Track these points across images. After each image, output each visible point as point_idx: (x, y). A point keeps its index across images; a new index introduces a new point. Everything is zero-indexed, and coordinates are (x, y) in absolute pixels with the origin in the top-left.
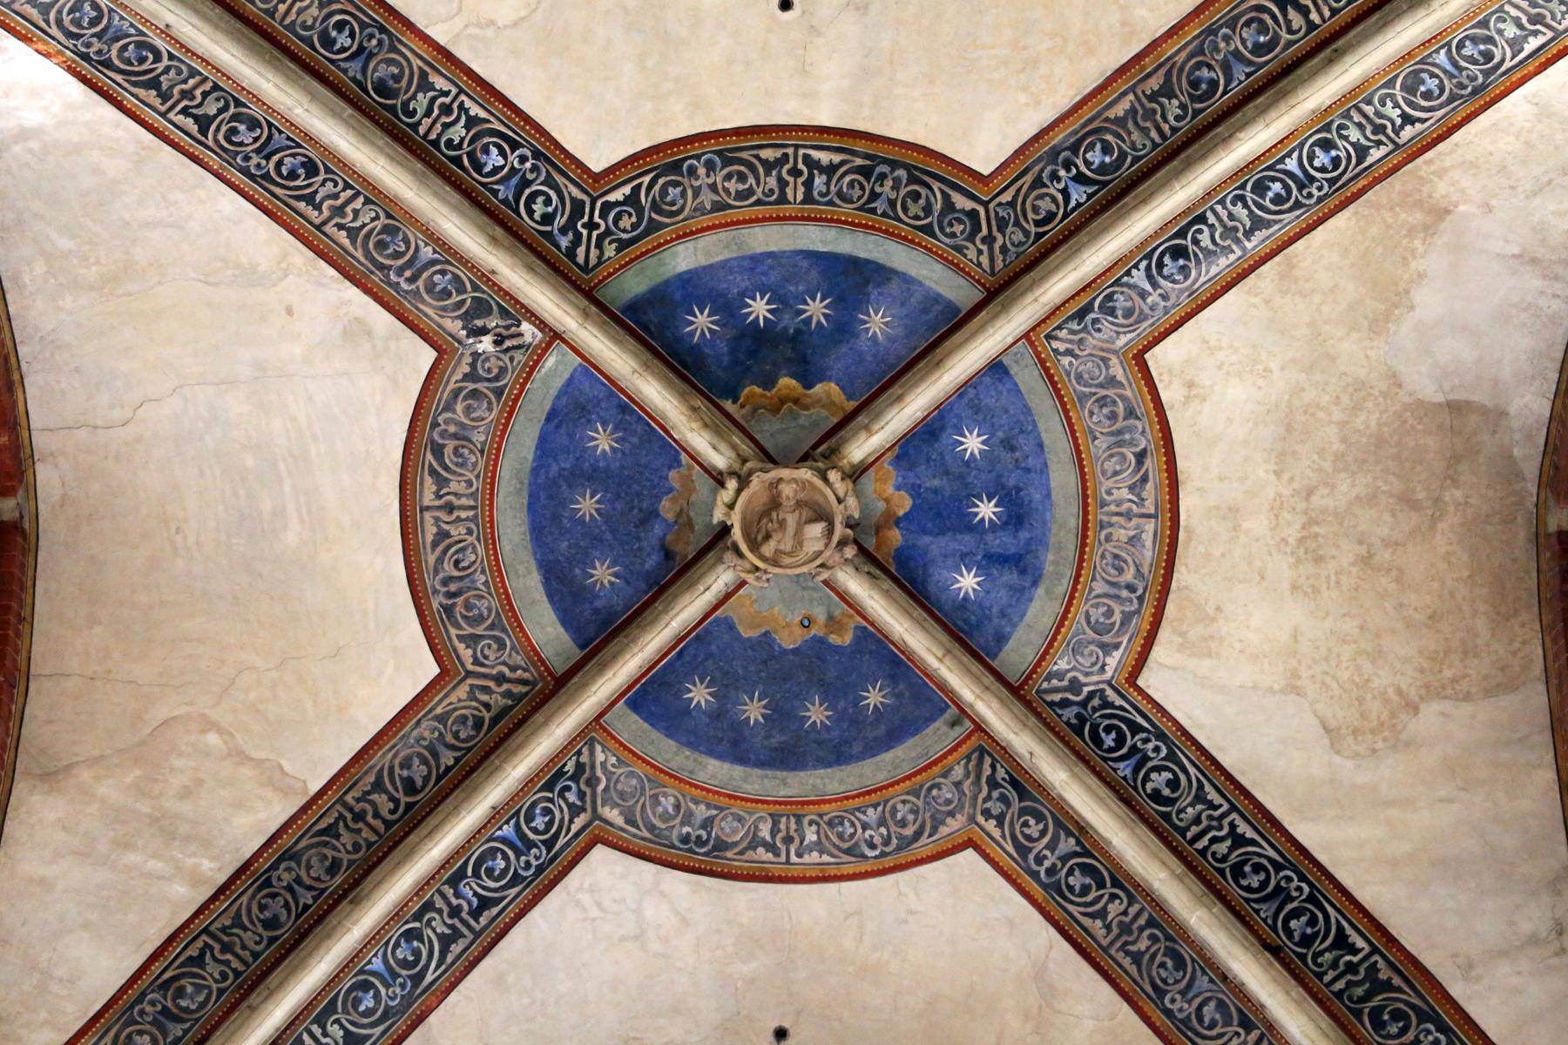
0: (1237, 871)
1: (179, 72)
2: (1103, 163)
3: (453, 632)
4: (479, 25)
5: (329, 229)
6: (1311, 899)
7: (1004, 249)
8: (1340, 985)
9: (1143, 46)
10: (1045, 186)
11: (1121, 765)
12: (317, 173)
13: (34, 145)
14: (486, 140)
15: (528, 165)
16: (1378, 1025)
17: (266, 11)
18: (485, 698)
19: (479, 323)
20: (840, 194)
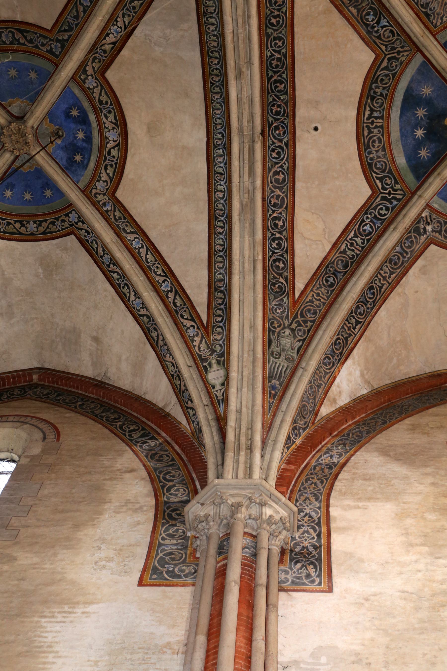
1: (343, 331)
2: (373, 15)
4: (325, 234)
5: (390, 281)
7: (402, 47)
9: (332, 6)
10: (380, 35)
12: (373, 286)
13: (365, 372)
14: (361, 231)
15: (369, 216)
17: (324, 305)
19: (422, 230)
20: (380, 107)
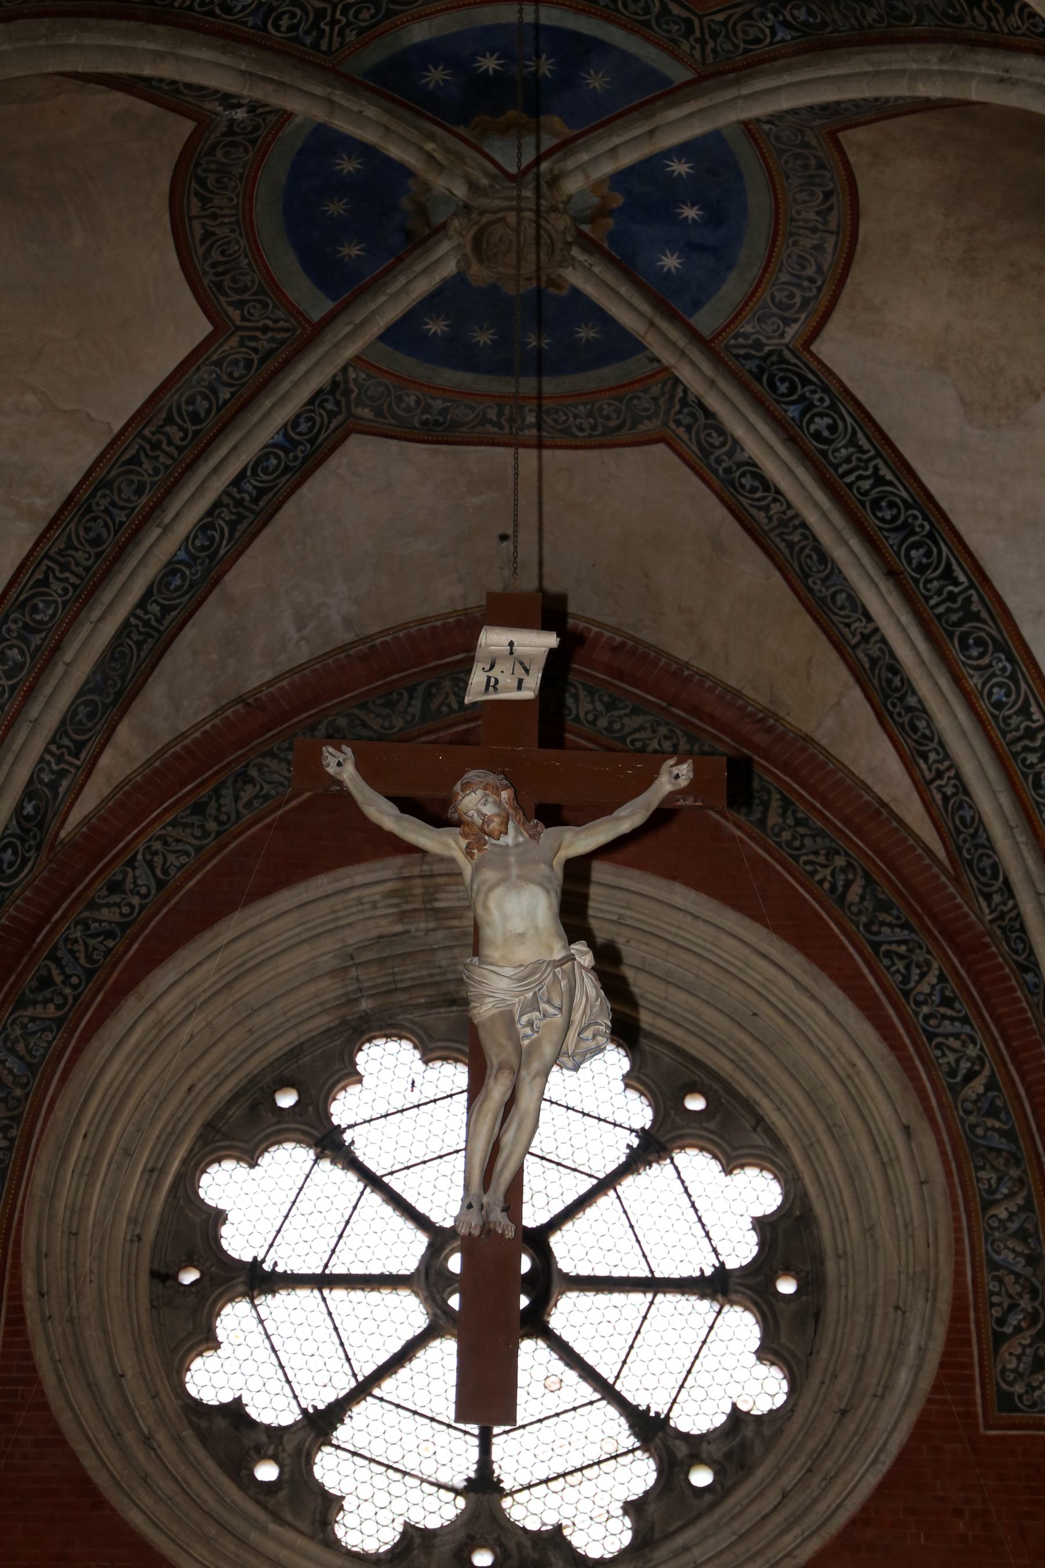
0: (875, 505)
3: (223, 299)
6: (930, 536)
7: (714, 51)
8: (941, 609)
10: (753, 19)
11: (792, 408)
16: (964, 647)
18: (253, 344)
